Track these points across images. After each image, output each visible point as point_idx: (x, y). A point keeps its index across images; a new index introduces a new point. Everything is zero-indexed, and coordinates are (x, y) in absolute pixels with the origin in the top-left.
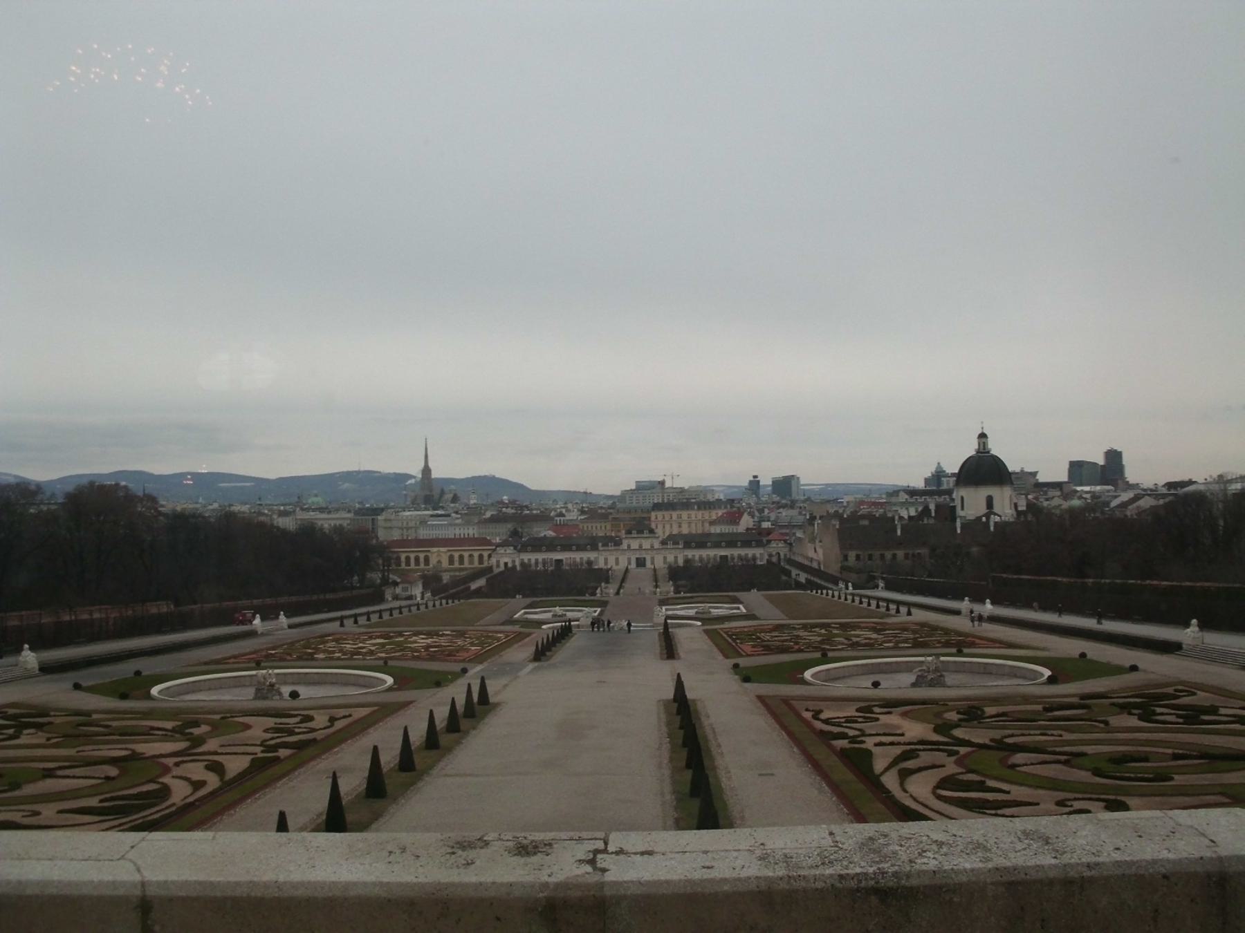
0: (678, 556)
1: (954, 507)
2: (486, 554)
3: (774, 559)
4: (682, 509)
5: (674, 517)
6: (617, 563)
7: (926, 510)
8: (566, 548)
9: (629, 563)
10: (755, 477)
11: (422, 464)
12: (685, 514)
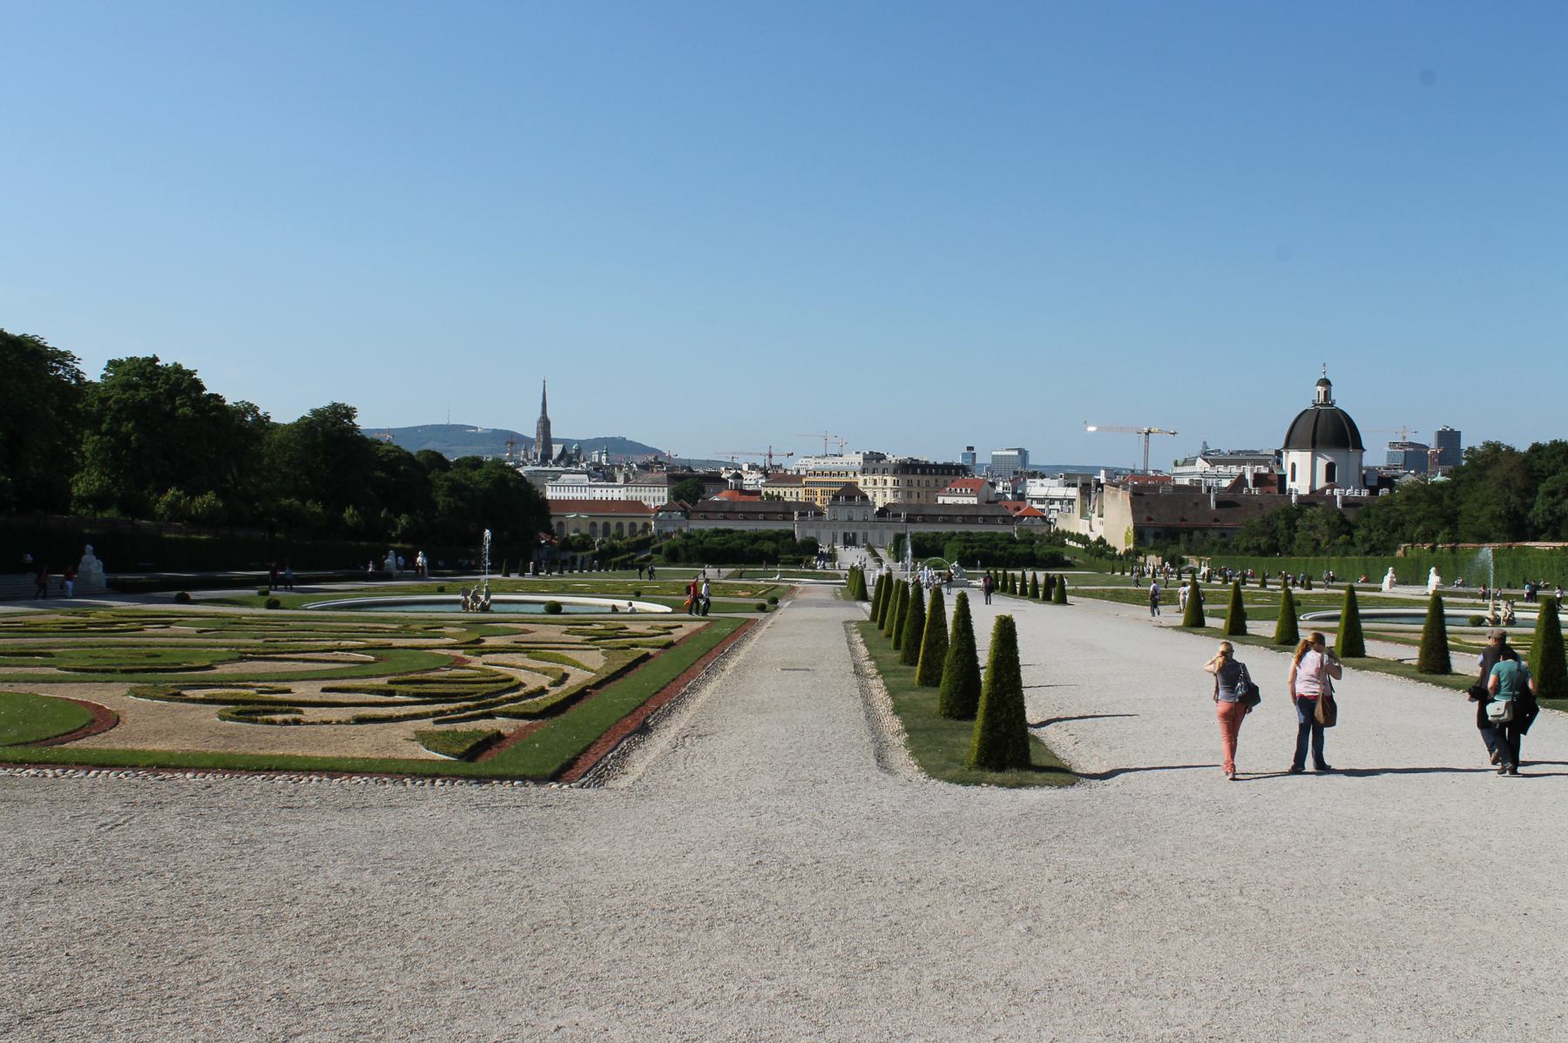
1: (1282, 478)
10: (971, 448)
11: (539, 415)
12: (903, 479)
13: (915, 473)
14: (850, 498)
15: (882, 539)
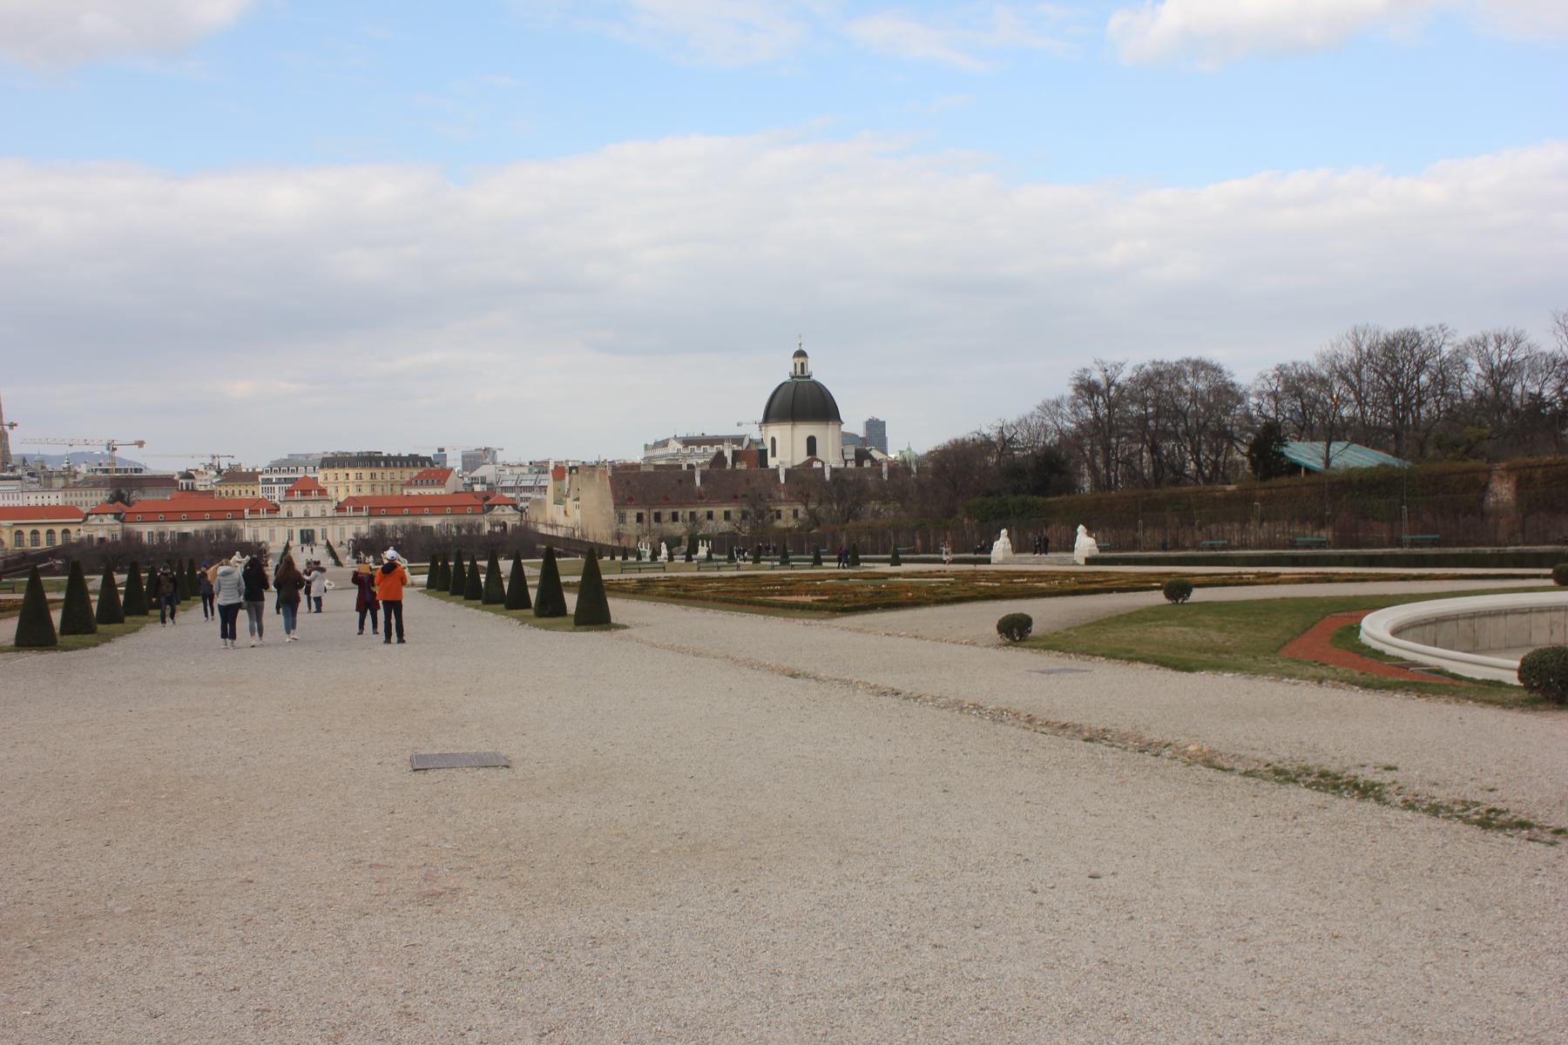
0: (364, 527)
2: (73, 529)
3: (497, 529)
4: (364, 466)
5: (352, 477)
6: (272, 536)
7: (720, 454)
8: (194, 516)
9: (291, 537)
10: (441, 450)
12: (366, 473)
13: (378, 466)
14: (304, 493)
15: (342, 533)
